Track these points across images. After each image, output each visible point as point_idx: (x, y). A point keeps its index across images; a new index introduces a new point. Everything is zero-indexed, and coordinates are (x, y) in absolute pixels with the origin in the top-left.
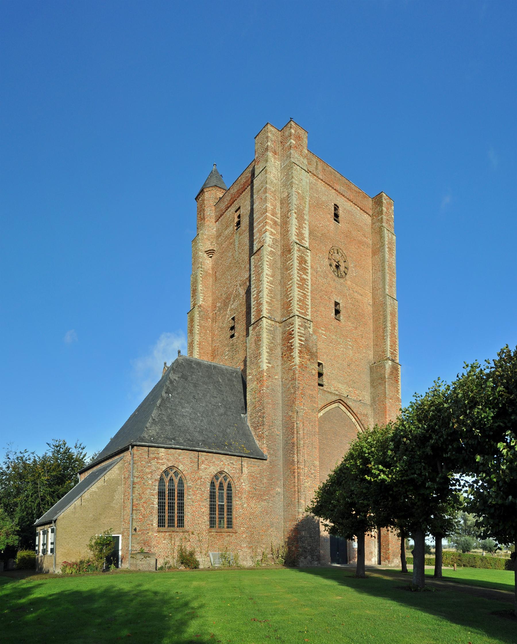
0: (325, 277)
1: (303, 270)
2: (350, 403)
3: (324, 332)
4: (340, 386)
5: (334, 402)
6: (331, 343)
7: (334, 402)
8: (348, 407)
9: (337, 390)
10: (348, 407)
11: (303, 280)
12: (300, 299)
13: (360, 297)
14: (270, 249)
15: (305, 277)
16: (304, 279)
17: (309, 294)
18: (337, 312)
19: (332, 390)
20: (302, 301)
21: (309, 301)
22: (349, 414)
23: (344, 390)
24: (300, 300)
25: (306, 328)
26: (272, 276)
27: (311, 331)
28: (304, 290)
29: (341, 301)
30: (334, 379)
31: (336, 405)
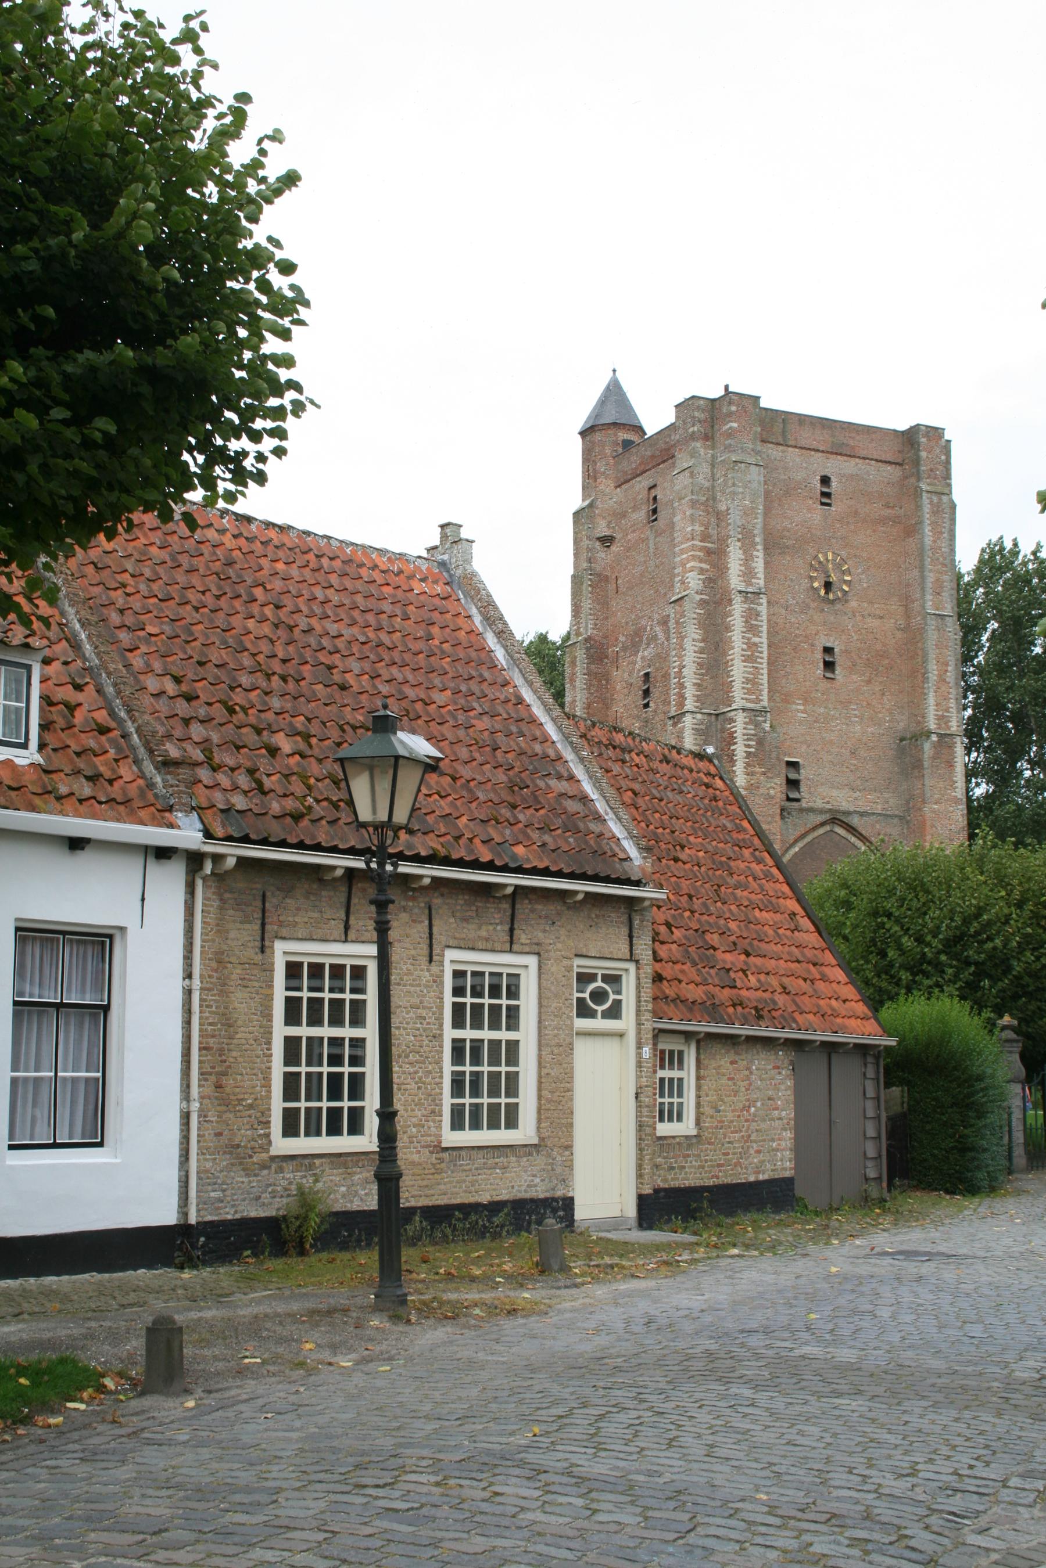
0: (805, 608)
1: (751, 628)
2: (855, 821)
3: (802, 708)
4: (835, 793)
5: (822, 824)
6: (815, 722)
7: (822, 824)
8: (851, 829)
9: (828, 802)
10: (851, 829)
11: (752, 646)
12: (747, 679)
13: (877, 622)
14: (698, 597)
15: (756, 640)
16: (755, 644)
17: (765, 666)
18: (829, 666)
19: (819, 804)
20: (752, 682)
21: (765, 677)
22: (853, 839)
23: (842, 800)
24: (748, 681)
25: (757, 725)
26: (703, 641)
27: (767, 726)
28: (756, 662)
29: (837, 643)
30: (822, 784)
31: (828, 828)
